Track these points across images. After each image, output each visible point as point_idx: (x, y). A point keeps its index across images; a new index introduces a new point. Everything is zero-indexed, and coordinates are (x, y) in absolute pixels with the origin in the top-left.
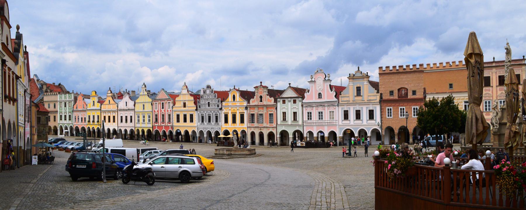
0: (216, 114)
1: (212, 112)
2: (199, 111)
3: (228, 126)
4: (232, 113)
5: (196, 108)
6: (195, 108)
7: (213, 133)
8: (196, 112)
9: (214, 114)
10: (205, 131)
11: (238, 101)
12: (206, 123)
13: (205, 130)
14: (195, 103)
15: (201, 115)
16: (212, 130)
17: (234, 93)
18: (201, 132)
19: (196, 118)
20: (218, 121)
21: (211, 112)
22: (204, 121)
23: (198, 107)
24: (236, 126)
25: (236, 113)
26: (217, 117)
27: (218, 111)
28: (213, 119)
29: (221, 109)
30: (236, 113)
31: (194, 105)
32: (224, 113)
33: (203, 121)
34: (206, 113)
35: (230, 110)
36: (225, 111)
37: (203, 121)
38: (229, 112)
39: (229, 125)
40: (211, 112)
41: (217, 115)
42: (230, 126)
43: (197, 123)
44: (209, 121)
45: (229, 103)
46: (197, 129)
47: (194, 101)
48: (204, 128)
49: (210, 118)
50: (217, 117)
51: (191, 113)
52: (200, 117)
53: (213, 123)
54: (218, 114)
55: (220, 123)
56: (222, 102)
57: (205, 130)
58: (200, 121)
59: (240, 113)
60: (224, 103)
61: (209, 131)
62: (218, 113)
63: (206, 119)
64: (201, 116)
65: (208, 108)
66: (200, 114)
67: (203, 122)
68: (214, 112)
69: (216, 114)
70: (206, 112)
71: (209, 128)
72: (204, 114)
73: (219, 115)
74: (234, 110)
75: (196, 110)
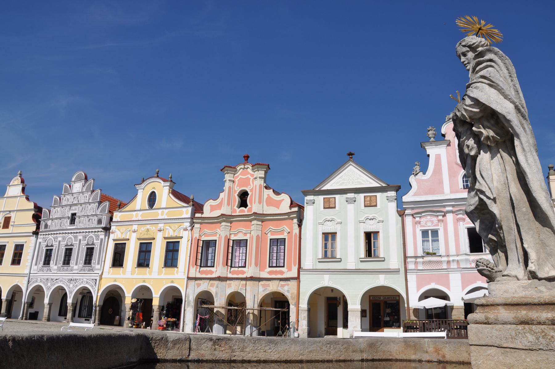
0: (90, 243)
1: (80, 237)
2: (42, 236)
3: (122, 276)
4: (139, 239)
5: (35, 230)
6: (34, 228)
7: (71, 293)
8: (33, 238)
9: (84, 242)
10: (48, 289)
11: (164, 205)
12: (56, 267)
13: (49, 284)
14: (37, 218)
15: (47, 246)
16: (71, 286)
17: (154, 188)
18: (38, 291)
19: (31, 254)
20: (93, 261)
21: (76, 237)
22: (51, 262)
23: (42, 228)
24: (147, 276)
25: (154, 239)
26: (90, 252)
27: (97, 237)
28: (79, 255)
29: (107, 229)
30: (154, 239)
31: (32, 222)
32: (114, 240)
33: (47, 262)
34: (60, 242)
35: (134, 232)
36: (117, 233)
37: (47, 262)
38: (130, 235)
39: (124, 273)
40: (76, 237)
41: (93, 244)
42: (128, 275)
43: (29, 268)
44: (67, 261)
45: (134, 213)
46: (26, 282)
47: (33, 212)
48: (47, 279)
49: (69, 252)
50: (90, 252)
51: (20, 241)
52: (43, 250)
53: (76, 267)
54: (97, 243)
55: (98, 267)
56: (111, 212)
57: (49, 284)
58: (40, 261)
59: (165, 238)
60: (117, 216)
61: (62, 289)
62: (97, 239)
63: (58, 255)
64: (45, 249)
65: (69, 228)
66: (44, 244)
67: (49, 264)
68: (85, 237)
69: (90, 243)
70: (60, 239)
71: (61, 281)
72: (56, 244)
73: (97, 247)
74: (148, 230)
75: (36, 233)
